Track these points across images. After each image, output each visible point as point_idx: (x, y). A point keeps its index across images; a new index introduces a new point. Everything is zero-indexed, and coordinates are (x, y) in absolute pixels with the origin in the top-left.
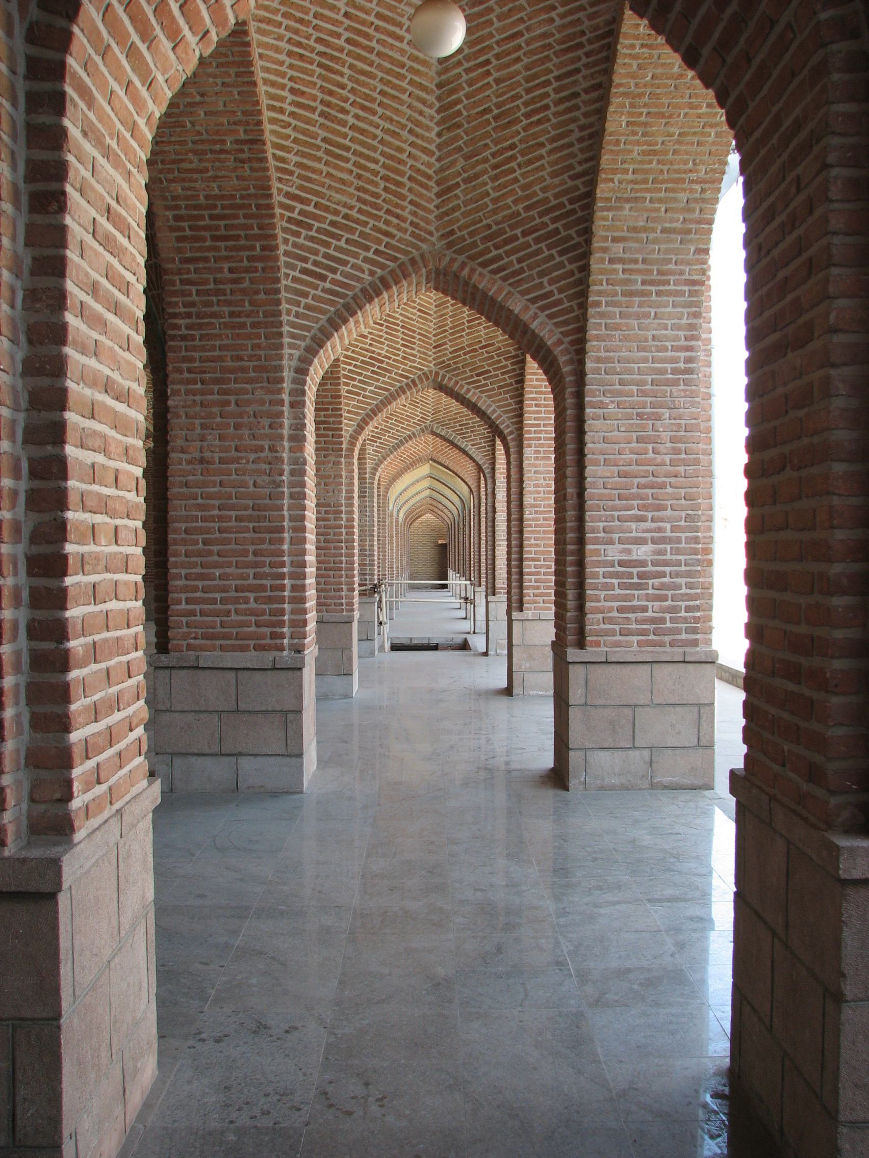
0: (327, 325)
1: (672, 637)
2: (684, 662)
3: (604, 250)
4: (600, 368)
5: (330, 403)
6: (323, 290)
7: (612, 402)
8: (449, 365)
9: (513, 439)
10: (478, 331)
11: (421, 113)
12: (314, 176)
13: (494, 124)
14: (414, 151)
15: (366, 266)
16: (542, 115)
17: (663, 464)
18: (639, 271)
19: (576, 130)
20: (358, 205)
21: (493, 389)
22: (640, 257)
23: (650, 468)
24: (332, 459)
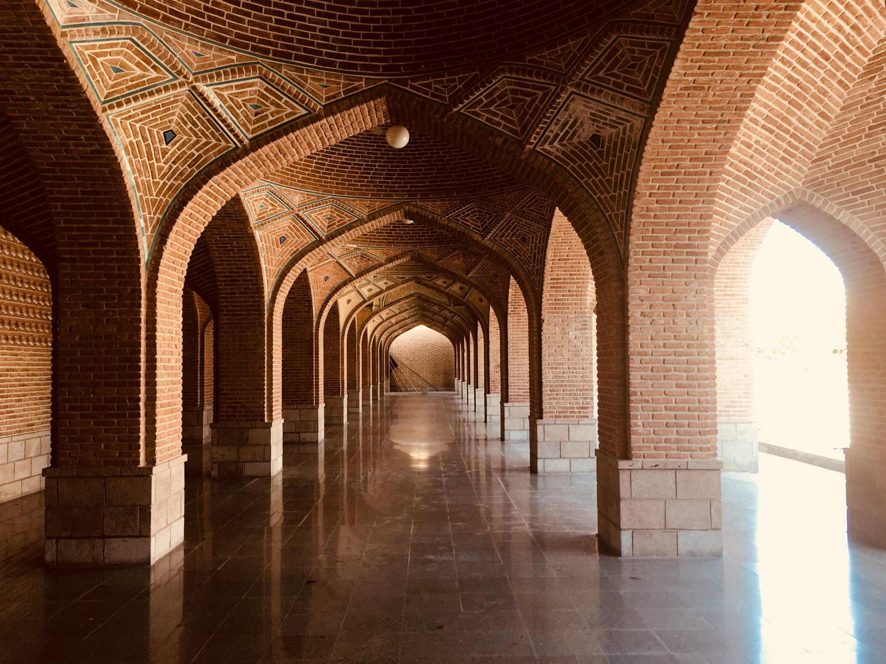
5: (698, 224)
8: (822, 183)
24: (695, 286)
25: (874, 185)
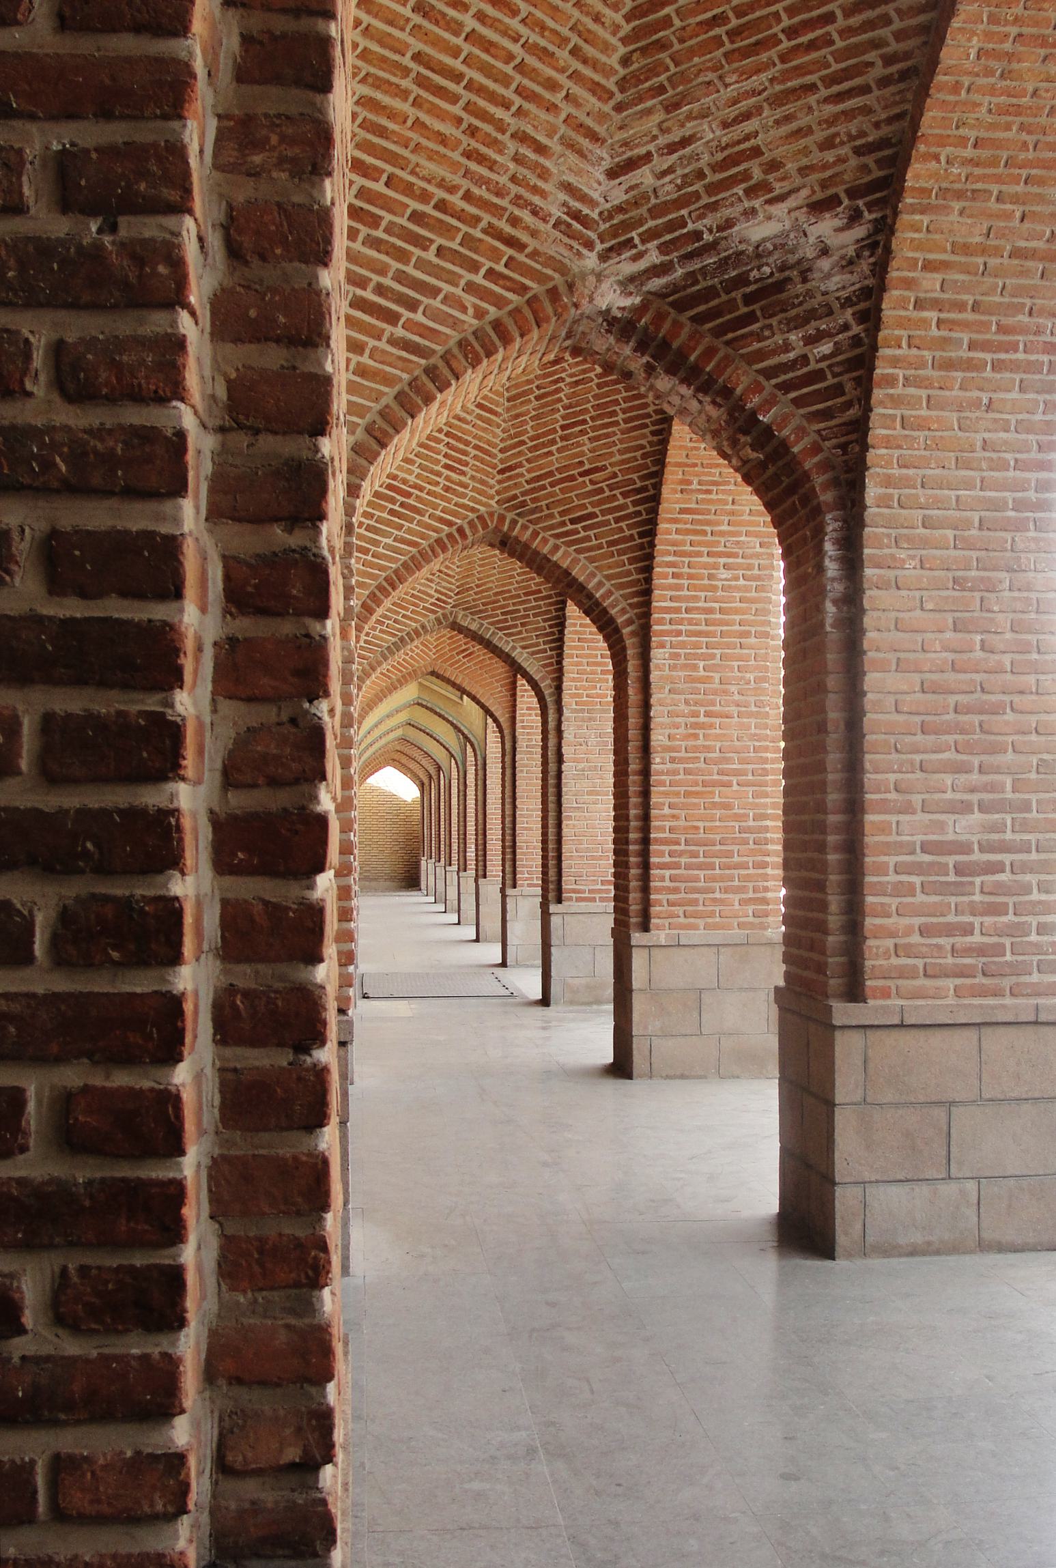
0: (395, 407)
1: (1014, 979)
2: (1036, 1023)
3: (908, 284)
4: (891, 497)
6: (392, 341)
7: (912, 557)
8: (523, 504)
9: (633, 633)
10: (579, 445)
11: (597, 18)
12: (391, 126)
13: (728, 46)
14: (577, 90)
15: (469, 300)
16: (819, 32)
17: (999, 670)
18: (965, 325)
19: (880, 63)
20: (466, 184)
21: (600, 547)
22: (969, 298)
23: (978, 677)
25: (596, 510)
